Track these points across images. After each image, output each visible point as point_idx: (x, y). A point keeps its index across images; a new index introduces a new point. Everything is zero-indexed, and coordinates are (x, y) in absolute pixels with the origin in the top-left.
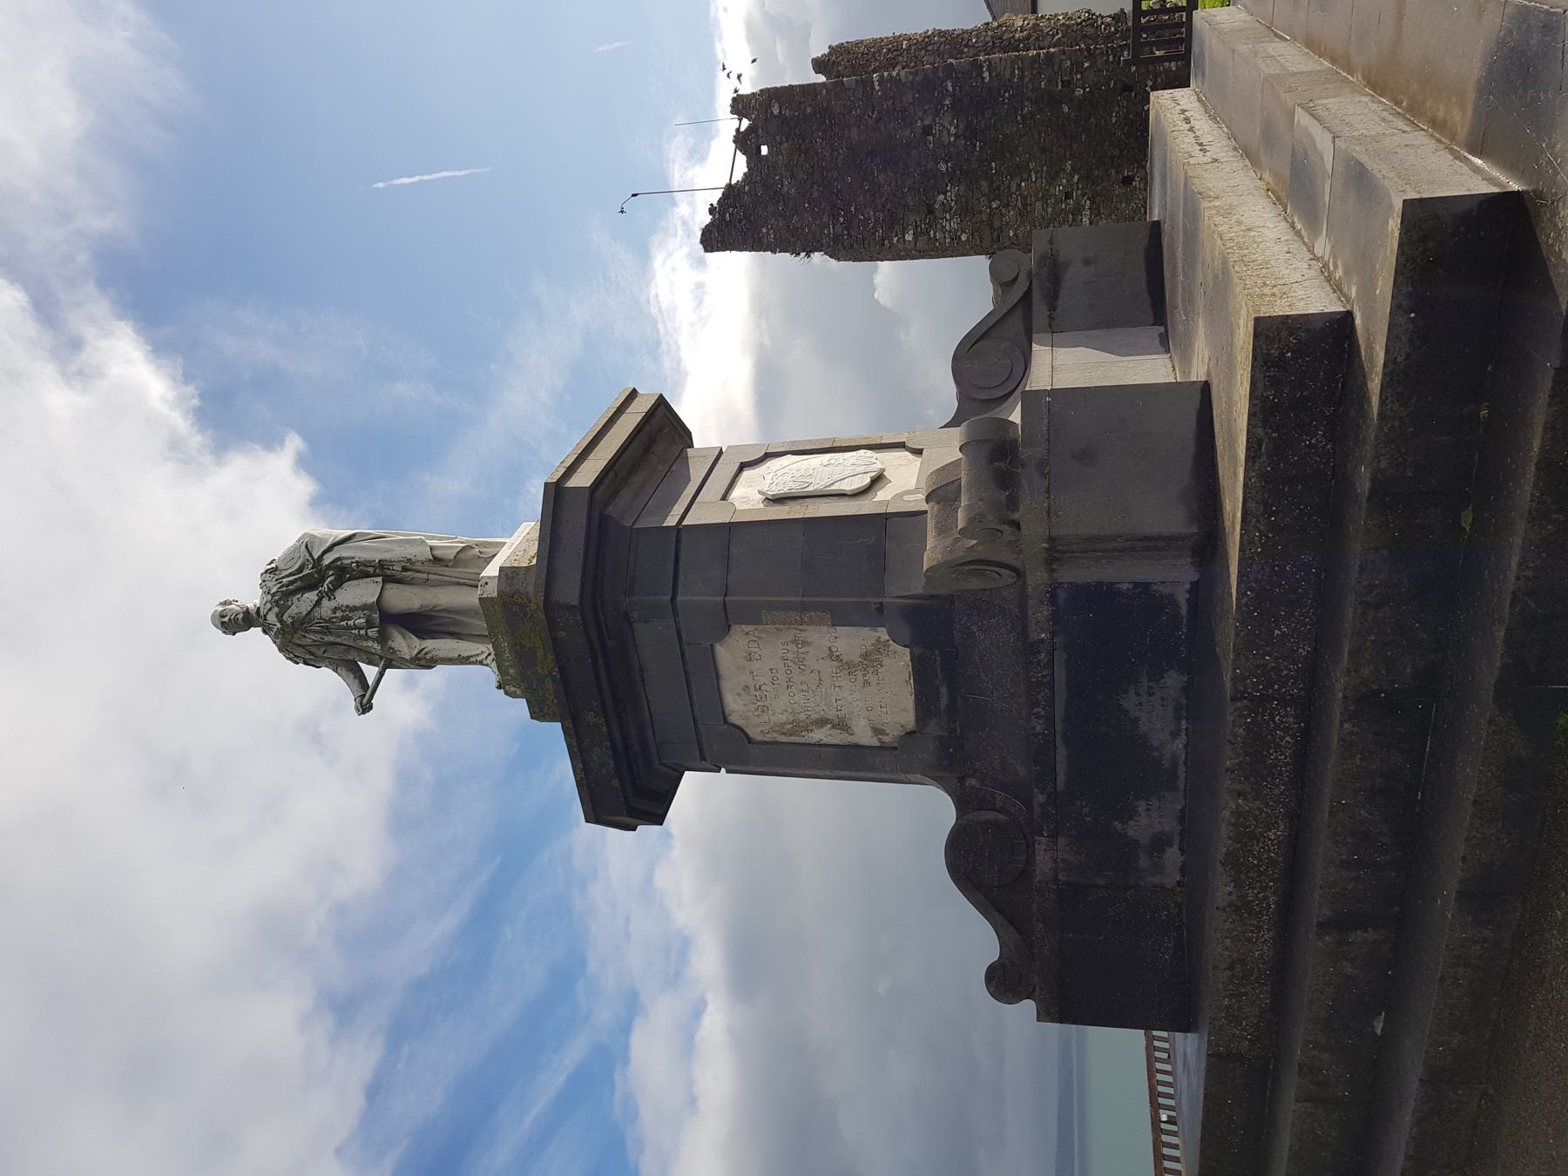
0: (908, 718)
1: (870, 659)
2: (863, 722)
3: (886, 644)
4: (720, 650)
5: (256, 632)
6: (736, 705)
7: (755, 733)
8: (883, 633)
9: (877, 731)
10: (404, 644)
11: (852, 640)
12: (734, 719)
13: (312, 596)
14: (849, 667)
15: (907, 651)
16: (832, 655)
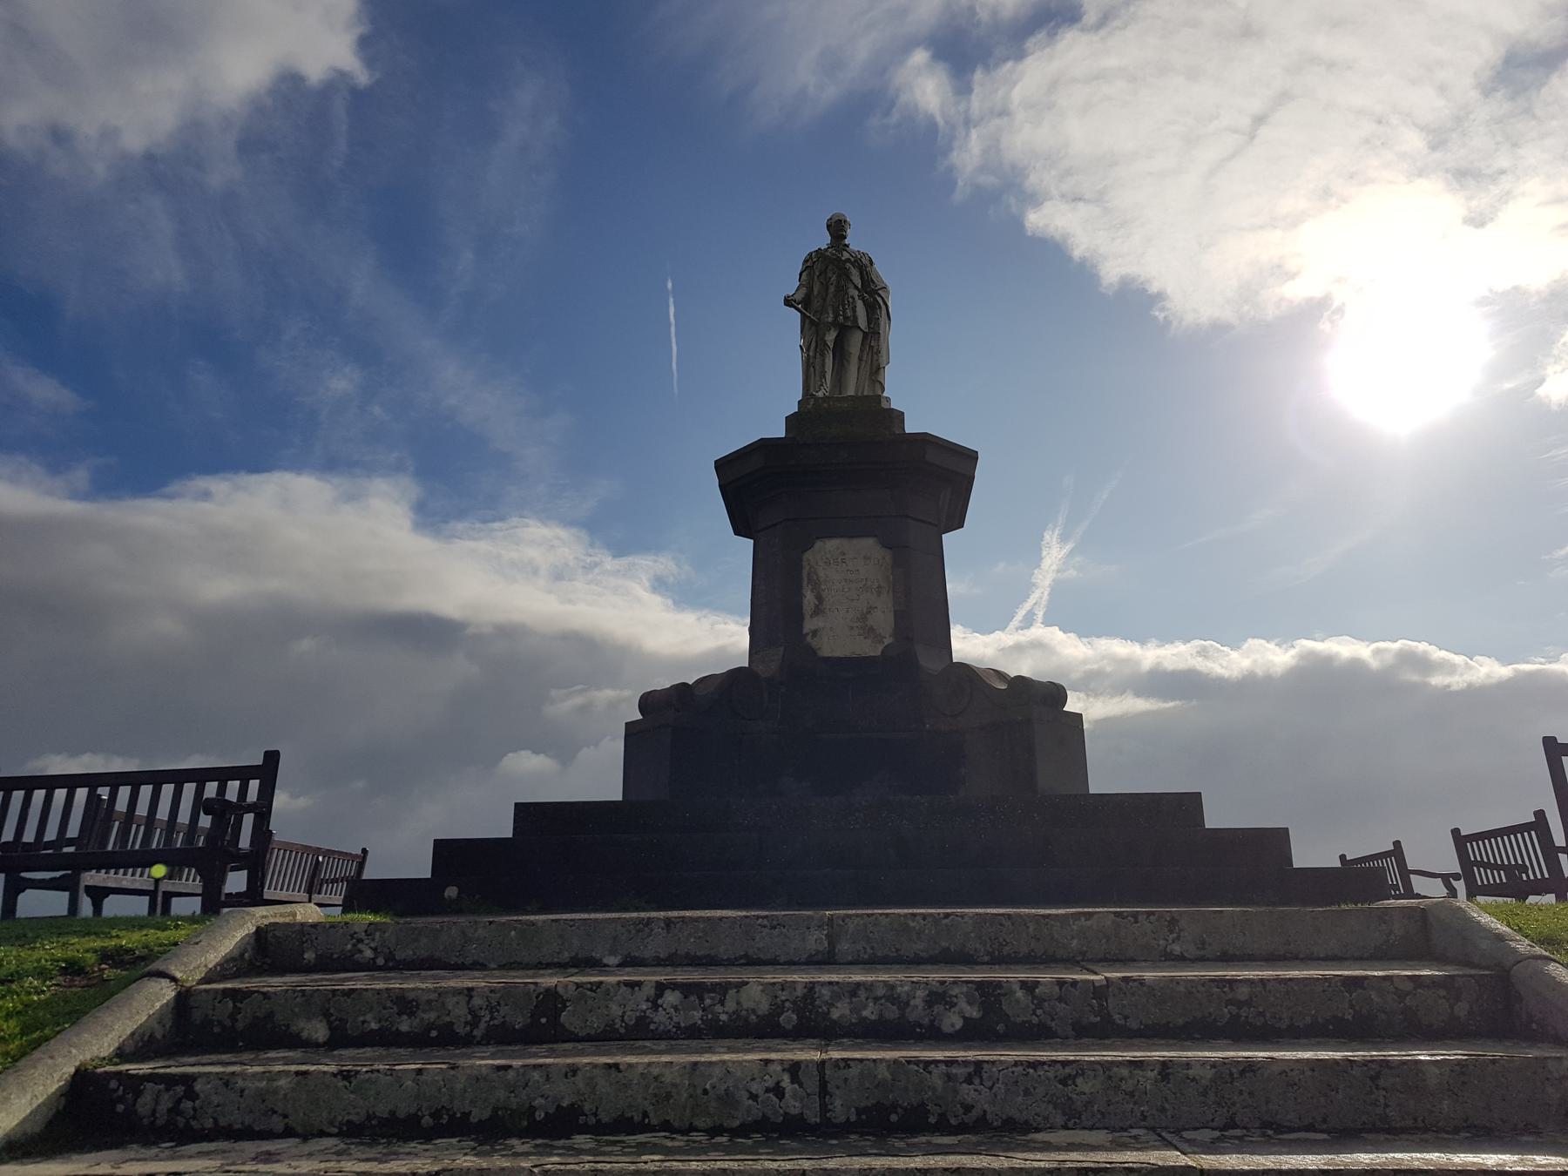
0: (826, 652)
1: (870, 632)
2: (821, 624)
3: (881, 642)
4: (870, 541)
5: (828, 239)
6: (832, 545)
7: (807, 555)
8: (887, 641)
9: (815, 633)
10: (831, 337)
11: (884, 620)
12: (818, 544)
13: (858, 282)
14: (863, 617)
15: (878, 653)
16: (871, 609)
